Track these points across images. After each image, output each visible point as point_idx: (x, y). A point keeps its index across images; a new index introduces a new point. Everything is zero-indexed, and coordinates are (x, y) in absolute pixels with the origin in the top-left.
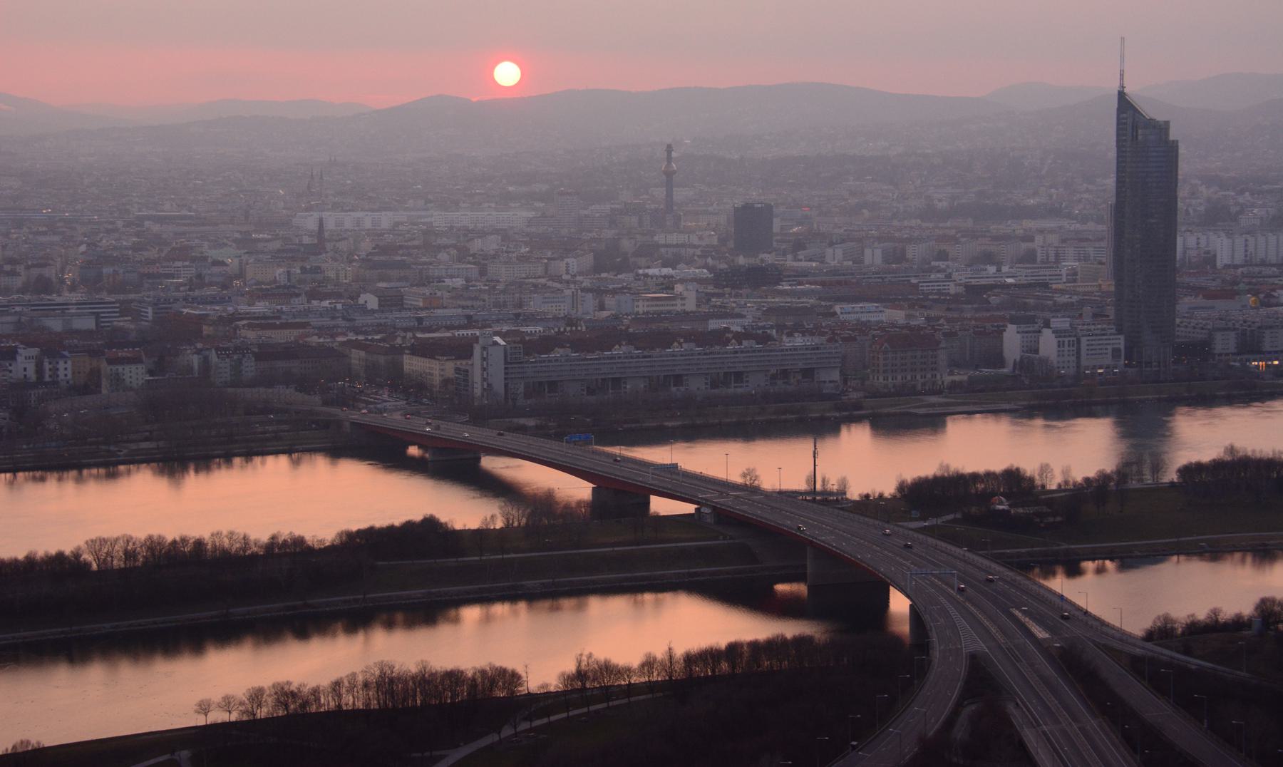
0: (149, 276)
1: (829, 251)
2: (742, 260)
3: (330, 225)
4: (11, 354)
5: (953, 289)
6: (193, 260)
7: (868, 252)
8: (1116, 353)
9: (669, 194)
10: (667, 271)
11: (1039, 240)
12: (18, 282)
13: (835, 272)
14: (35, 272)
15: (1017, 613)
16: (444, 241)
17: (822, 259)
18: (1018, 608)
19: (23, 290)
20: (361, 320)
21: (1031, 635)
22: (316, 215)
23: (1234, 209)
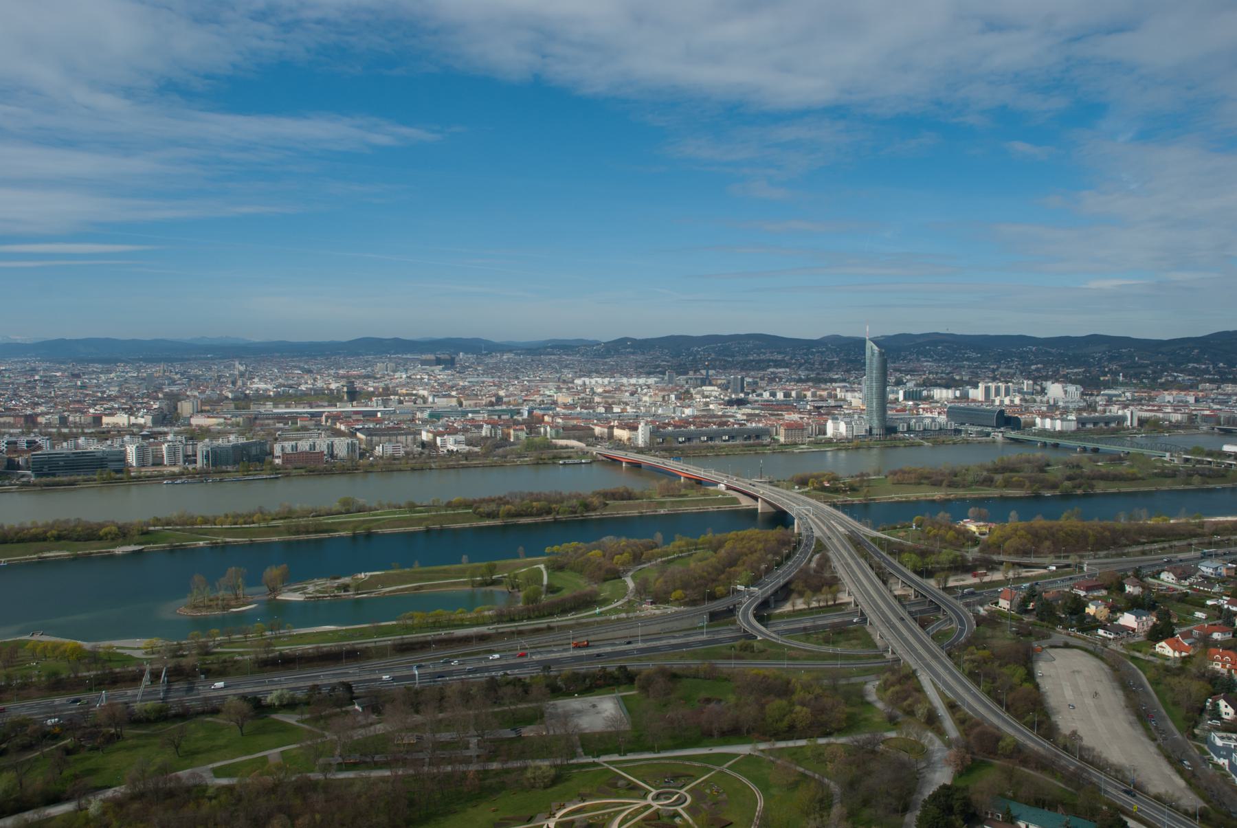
0: (525, 400)
1: (764, 393)
2: (733, 396)
3: (587, 383)
4: (481, 427)
5: (808, 407)
6: (542, 395)
7: (778, 394)
8: (866, 430)
9: (707, 373)
10: (708, 400)
11: (838, 390)
12: (484, 402)
13: (767, 401)
14: (489, 399)
15: (833, 522)
16: (627, 388)
17: (761, 395)
18: (833, 520)
19: (485, 405)
20: (600, 417)
21: (838, 530)
22: (583, 379)
23: (905, 381)
